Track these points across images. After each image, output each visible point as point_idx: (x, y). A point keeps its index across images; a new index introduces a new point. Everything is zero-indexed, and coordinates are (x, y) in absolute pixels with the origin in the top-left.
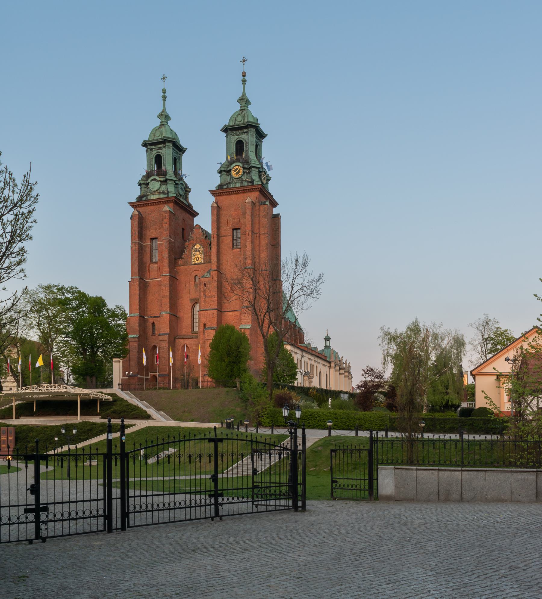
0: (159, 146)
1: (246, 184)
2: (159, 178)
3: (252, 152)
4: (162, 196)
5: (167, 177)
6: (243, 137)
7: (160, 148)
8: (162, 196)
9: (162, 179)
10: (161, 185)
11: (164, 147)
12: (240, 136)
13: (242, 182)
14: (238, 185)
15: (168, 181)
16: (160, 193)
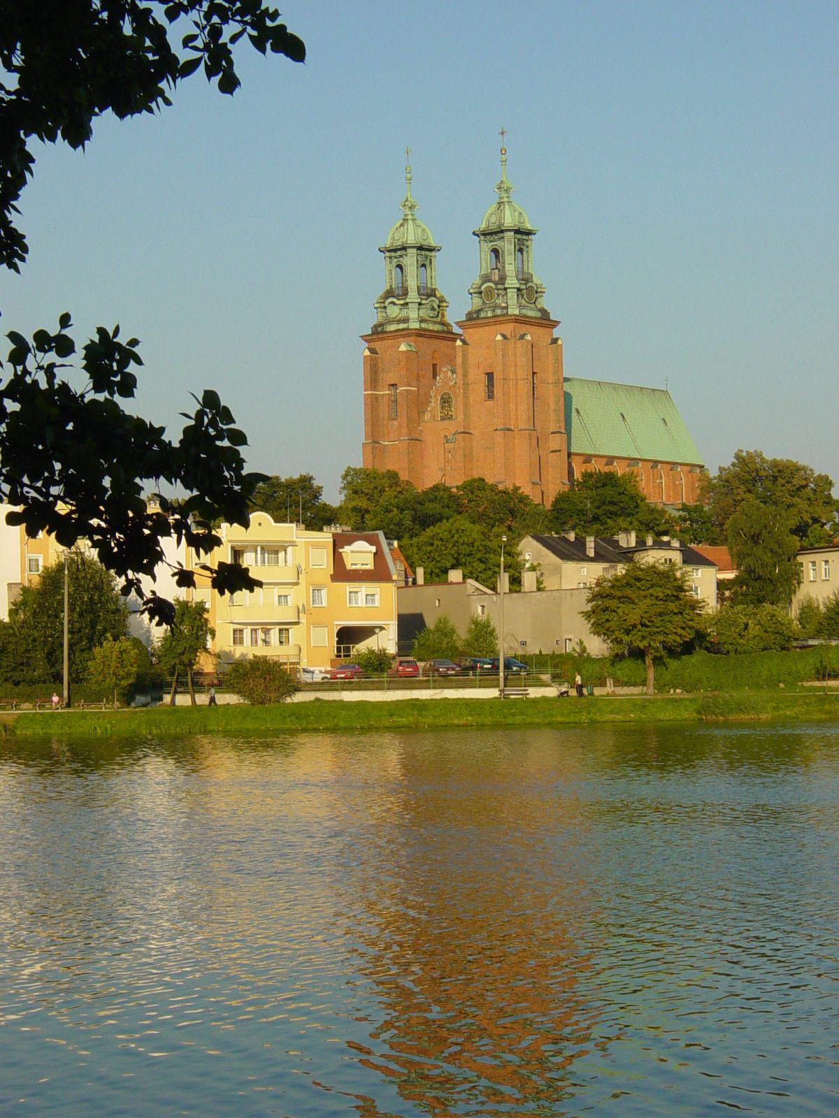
0: (399, 253)
1: (499, 312)
2: (398, 299)
3: (510, 264)
4: (401, 326)
5: (408, 300)
6: (498, 244)
7: (401, 256)
8: (401, 326)
9: (402, 302)
10: (401, 309)
11: (406, 255)
12: (495, 243)
13: (494, 310)
14: (490, 314)
15: (410, 305)
16: (399, 321)
